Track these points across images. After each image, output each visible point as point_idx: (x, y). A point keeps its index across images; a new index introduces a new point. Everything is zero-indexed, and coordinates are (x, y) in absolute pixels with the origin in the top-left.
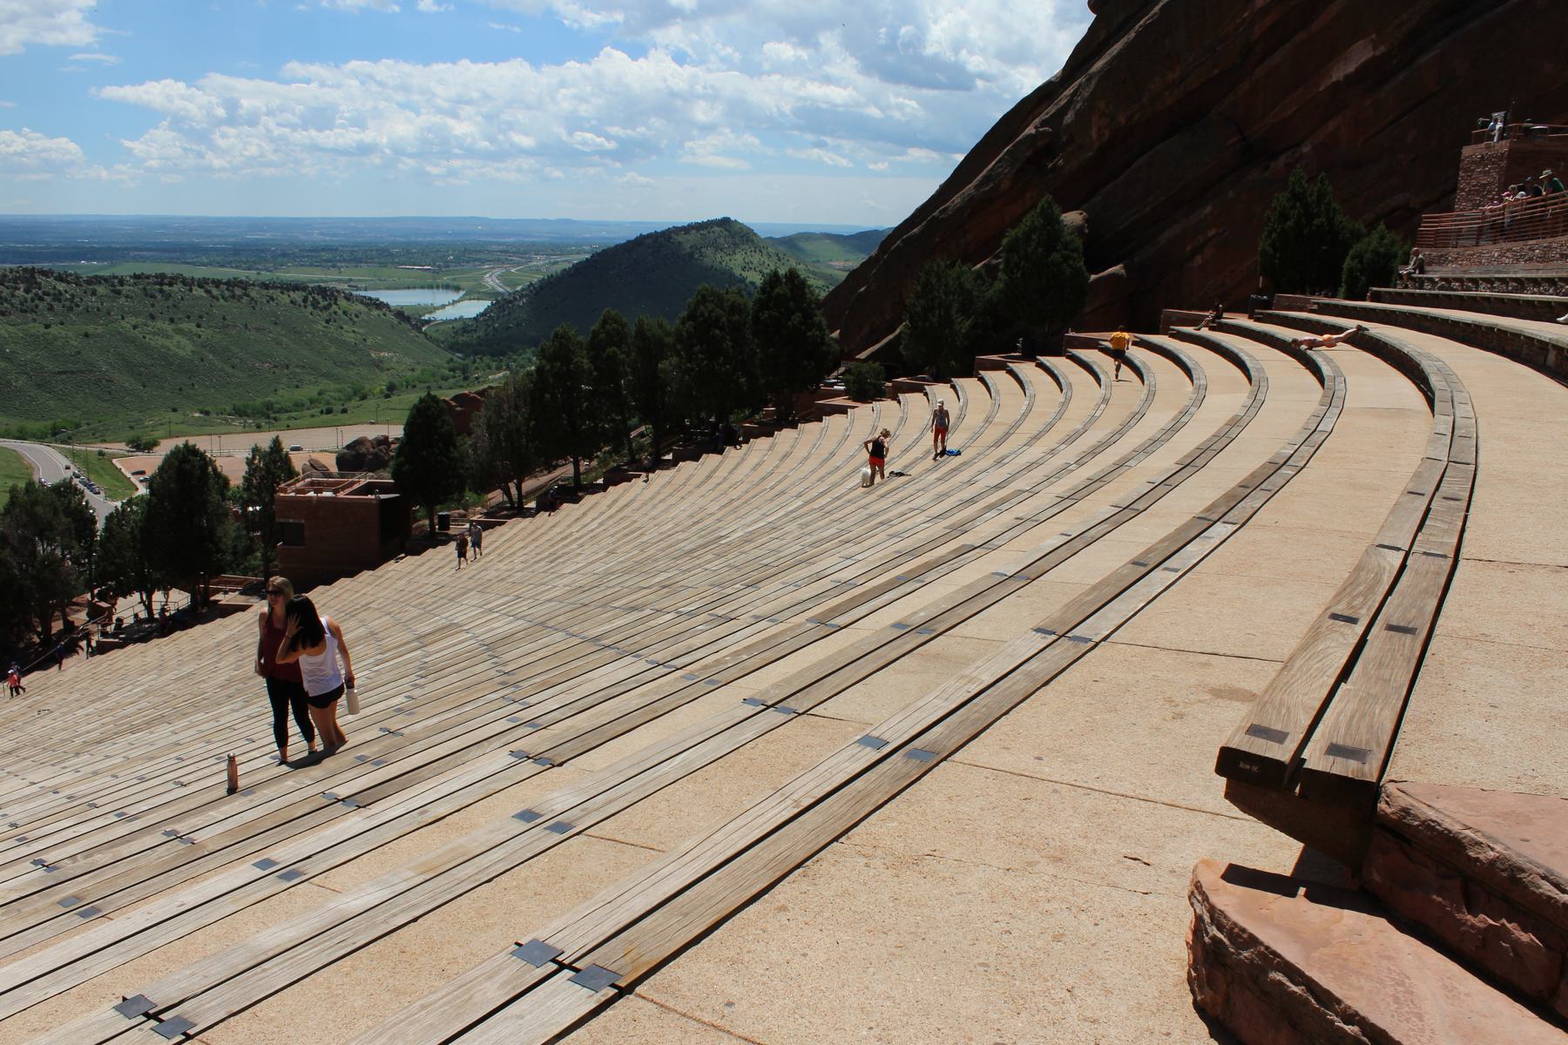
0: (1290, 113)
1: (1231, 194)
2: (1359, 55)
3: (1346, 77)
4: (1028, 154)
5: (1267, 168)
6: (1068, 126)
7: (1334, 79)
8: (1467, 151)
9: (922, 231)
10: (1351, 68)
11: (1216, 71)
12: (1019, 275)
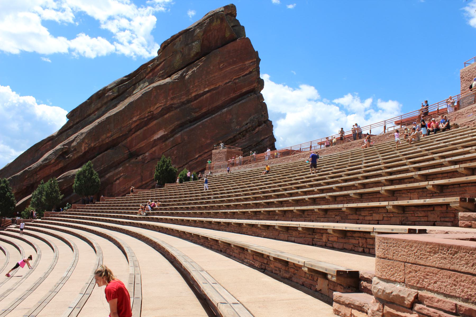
0: (143, 146)
1: (127, 165)
2: (161, 133)
3: (158, 138)
4: (61, 153)
5: (136, 159)
6: (74, 146)
7: (155, 138)
8: (213, 151)
9: (21, 174)
11: (121, 135)
12: (83, 182)
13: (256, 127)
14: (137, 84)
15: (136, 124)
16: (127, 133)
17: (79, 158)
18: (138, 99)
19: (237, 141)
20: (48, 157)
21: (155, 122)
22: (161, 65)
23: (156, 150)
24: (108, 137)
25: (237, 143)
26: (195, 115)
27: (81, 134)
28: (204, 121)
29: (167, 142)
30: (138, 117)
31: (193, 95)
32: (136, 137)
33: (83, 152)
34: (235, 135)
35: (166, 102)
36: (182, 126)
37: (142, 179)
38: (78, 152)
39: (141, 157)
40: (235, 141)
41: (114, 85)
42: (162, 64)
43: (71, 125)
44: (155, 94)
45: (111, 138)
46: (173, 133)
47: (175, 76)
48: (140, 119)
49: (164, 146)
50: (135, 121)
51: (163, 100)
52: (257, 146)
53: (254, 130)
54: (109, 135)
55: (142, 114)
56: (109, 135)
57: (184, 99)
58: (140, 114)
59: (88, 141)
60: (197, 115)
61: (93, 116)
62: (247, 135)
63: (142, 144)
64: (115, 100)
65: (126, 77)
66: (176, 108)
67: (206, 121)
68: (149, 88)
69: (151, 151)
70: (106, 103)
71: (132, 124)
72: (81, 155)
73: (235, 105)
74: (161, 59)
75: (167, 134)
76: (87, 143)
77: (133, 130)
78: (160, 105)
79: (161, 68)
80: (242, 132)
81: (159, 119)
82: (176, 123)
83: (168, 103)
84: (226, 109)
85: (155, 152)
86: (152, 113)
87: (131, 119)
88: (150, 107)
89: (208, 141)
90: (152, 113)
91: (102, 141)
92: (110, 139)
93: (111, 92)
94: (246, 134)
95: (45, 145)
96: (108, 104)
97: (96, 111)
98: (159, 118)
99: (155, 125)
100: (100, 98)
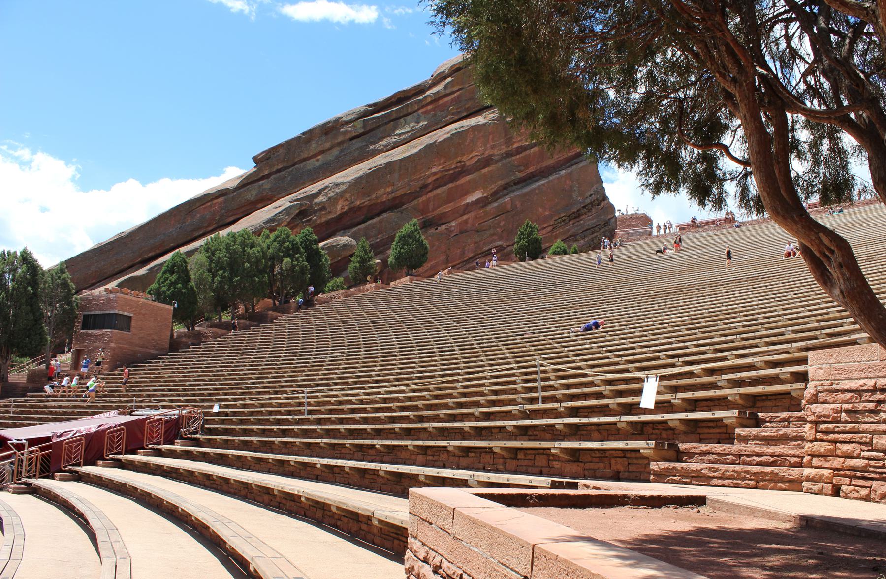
2: (477, 195)
5: (437, 229)
7: (468, 202)
10: (474, 199)
13: (601, 202)
14: (402, 120)
15: (435, 178)
16: (418, 189)
17: (328, 223)
18: (445, 140)
19: (582, 217)
20: (274, 216)
21: (468, 178)
22: (453, 96)
23: (469, 218)
24: (388, 193)
25: (581, 220)
26: (520, 175)
27: (336, 185)
28: (534, 186)
29: (489, 208)
30: (441, 167)
31: (515, 146)
32: (434, 196)
33: (338, 213)
34: (579, 208)
35: (485, 150)
37: (447, 259)
38: (330, 212)
39: (443, 227)
40: (579, 216)
41: (353, 117)
42: (456, 95)
43: (266, 172)
44: (471, 136)
45: (393, 195)
46: (495, 196)
47: (492, 115)
48: (443, 171)
49: (483, 214)
50: (435, 174)
51: (481, 147)
52: (605, 226)
53: (599, 204)
55: (447, 164)
56: (389, 189)
57: (504, 149)
58: (443, 164)
59: (351, 197)
60: (522, 175)
61: (312, 164)
62: (593, 210)
63: (447, 208)
64: (359, 139)
65: (369, 106)
66: (497, 161)
67: (543, 185)
68: (462, 127)
69: (460, 220)
70: (339, 144)
71: (429, 177)
72: (333, 218)
73: (574, 167)
74: (453, 86)
75: (486, 197)
76: (347, 200)
77: (431, 186)
78: (477, 153)
79: (452, 100)
80: (586, 206)
81: (474, 174)
82: (501, 183)
83: (487, 152)
84: (564, 172)
85: (466, 221)
86: (463, 164)
87: (429, 168)
88: (463, 155)
89: (547, 213)
90: (463, 164)
91: (377, 198)
92: (390, 196)
93: (350, 127)
94: (591, 209)
95: (209, 204)
96: (345, 145)
97: (320, 155)
98: (474, 172)
99: (469, 181)
100: (326, 134)
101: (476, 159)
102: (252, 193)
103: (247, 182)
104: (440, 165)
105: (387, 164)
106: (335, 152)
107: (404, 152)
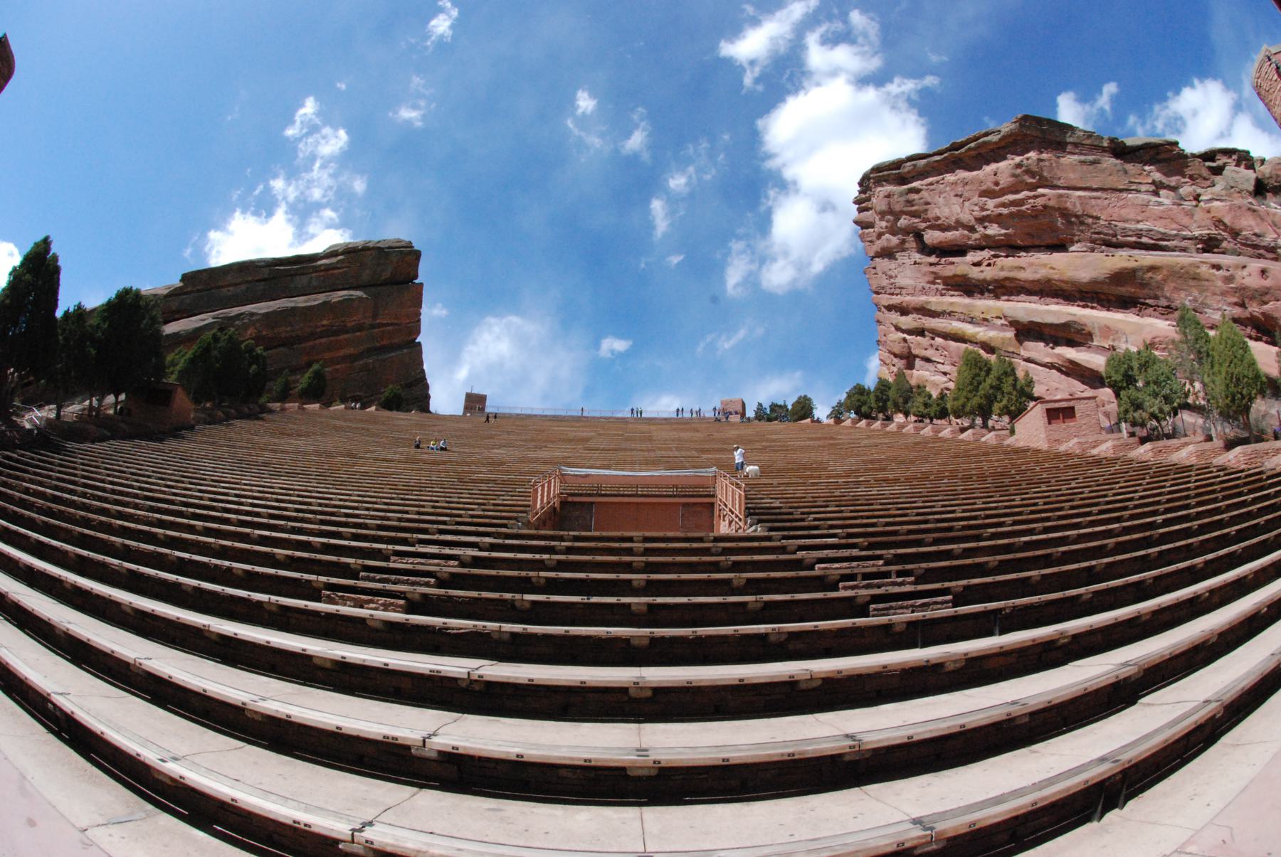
15: (323, 329)
21: (346, 336)
24: (287, 332)
31: (378, 321)
36: (370, 352)
43: (189, 289)
50: (323, 326)
54: (289, 329)
56: (289, 329)
101: (354, 323)
102: (174, 305)
103: (175, 293)
104: (329, 319)
105: (292, 308)
106: (243, 287)
107: (305, 302)
